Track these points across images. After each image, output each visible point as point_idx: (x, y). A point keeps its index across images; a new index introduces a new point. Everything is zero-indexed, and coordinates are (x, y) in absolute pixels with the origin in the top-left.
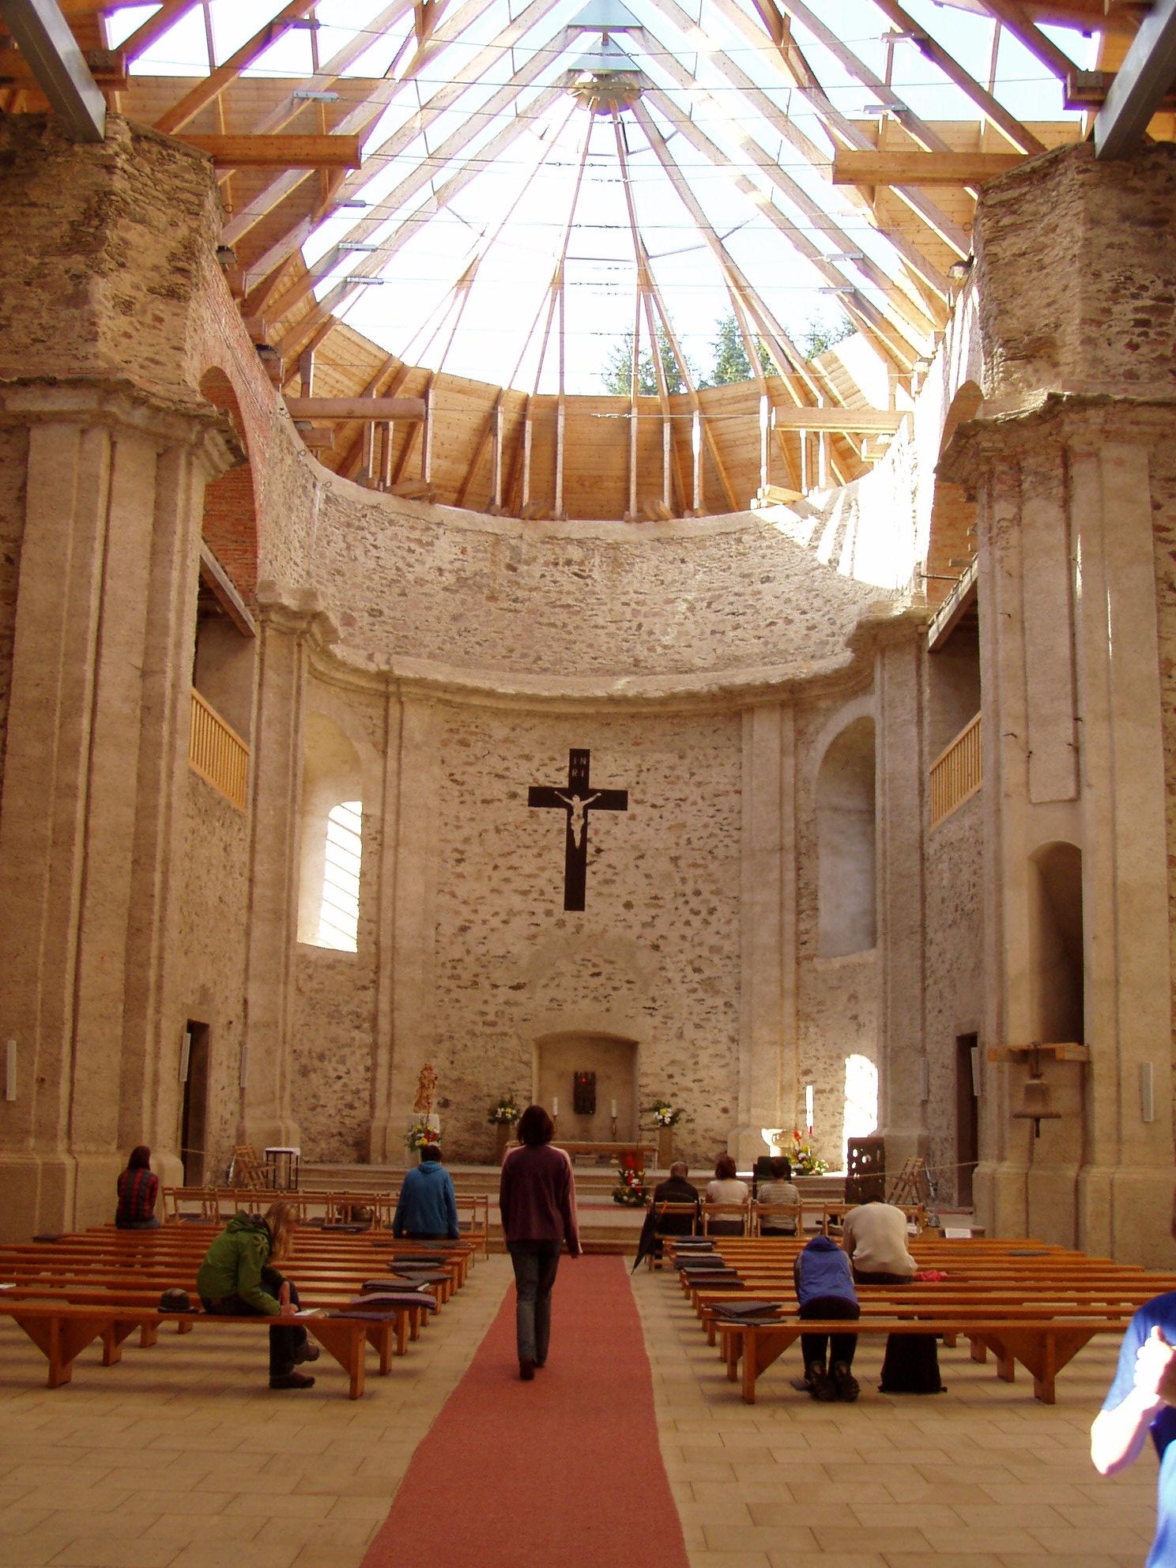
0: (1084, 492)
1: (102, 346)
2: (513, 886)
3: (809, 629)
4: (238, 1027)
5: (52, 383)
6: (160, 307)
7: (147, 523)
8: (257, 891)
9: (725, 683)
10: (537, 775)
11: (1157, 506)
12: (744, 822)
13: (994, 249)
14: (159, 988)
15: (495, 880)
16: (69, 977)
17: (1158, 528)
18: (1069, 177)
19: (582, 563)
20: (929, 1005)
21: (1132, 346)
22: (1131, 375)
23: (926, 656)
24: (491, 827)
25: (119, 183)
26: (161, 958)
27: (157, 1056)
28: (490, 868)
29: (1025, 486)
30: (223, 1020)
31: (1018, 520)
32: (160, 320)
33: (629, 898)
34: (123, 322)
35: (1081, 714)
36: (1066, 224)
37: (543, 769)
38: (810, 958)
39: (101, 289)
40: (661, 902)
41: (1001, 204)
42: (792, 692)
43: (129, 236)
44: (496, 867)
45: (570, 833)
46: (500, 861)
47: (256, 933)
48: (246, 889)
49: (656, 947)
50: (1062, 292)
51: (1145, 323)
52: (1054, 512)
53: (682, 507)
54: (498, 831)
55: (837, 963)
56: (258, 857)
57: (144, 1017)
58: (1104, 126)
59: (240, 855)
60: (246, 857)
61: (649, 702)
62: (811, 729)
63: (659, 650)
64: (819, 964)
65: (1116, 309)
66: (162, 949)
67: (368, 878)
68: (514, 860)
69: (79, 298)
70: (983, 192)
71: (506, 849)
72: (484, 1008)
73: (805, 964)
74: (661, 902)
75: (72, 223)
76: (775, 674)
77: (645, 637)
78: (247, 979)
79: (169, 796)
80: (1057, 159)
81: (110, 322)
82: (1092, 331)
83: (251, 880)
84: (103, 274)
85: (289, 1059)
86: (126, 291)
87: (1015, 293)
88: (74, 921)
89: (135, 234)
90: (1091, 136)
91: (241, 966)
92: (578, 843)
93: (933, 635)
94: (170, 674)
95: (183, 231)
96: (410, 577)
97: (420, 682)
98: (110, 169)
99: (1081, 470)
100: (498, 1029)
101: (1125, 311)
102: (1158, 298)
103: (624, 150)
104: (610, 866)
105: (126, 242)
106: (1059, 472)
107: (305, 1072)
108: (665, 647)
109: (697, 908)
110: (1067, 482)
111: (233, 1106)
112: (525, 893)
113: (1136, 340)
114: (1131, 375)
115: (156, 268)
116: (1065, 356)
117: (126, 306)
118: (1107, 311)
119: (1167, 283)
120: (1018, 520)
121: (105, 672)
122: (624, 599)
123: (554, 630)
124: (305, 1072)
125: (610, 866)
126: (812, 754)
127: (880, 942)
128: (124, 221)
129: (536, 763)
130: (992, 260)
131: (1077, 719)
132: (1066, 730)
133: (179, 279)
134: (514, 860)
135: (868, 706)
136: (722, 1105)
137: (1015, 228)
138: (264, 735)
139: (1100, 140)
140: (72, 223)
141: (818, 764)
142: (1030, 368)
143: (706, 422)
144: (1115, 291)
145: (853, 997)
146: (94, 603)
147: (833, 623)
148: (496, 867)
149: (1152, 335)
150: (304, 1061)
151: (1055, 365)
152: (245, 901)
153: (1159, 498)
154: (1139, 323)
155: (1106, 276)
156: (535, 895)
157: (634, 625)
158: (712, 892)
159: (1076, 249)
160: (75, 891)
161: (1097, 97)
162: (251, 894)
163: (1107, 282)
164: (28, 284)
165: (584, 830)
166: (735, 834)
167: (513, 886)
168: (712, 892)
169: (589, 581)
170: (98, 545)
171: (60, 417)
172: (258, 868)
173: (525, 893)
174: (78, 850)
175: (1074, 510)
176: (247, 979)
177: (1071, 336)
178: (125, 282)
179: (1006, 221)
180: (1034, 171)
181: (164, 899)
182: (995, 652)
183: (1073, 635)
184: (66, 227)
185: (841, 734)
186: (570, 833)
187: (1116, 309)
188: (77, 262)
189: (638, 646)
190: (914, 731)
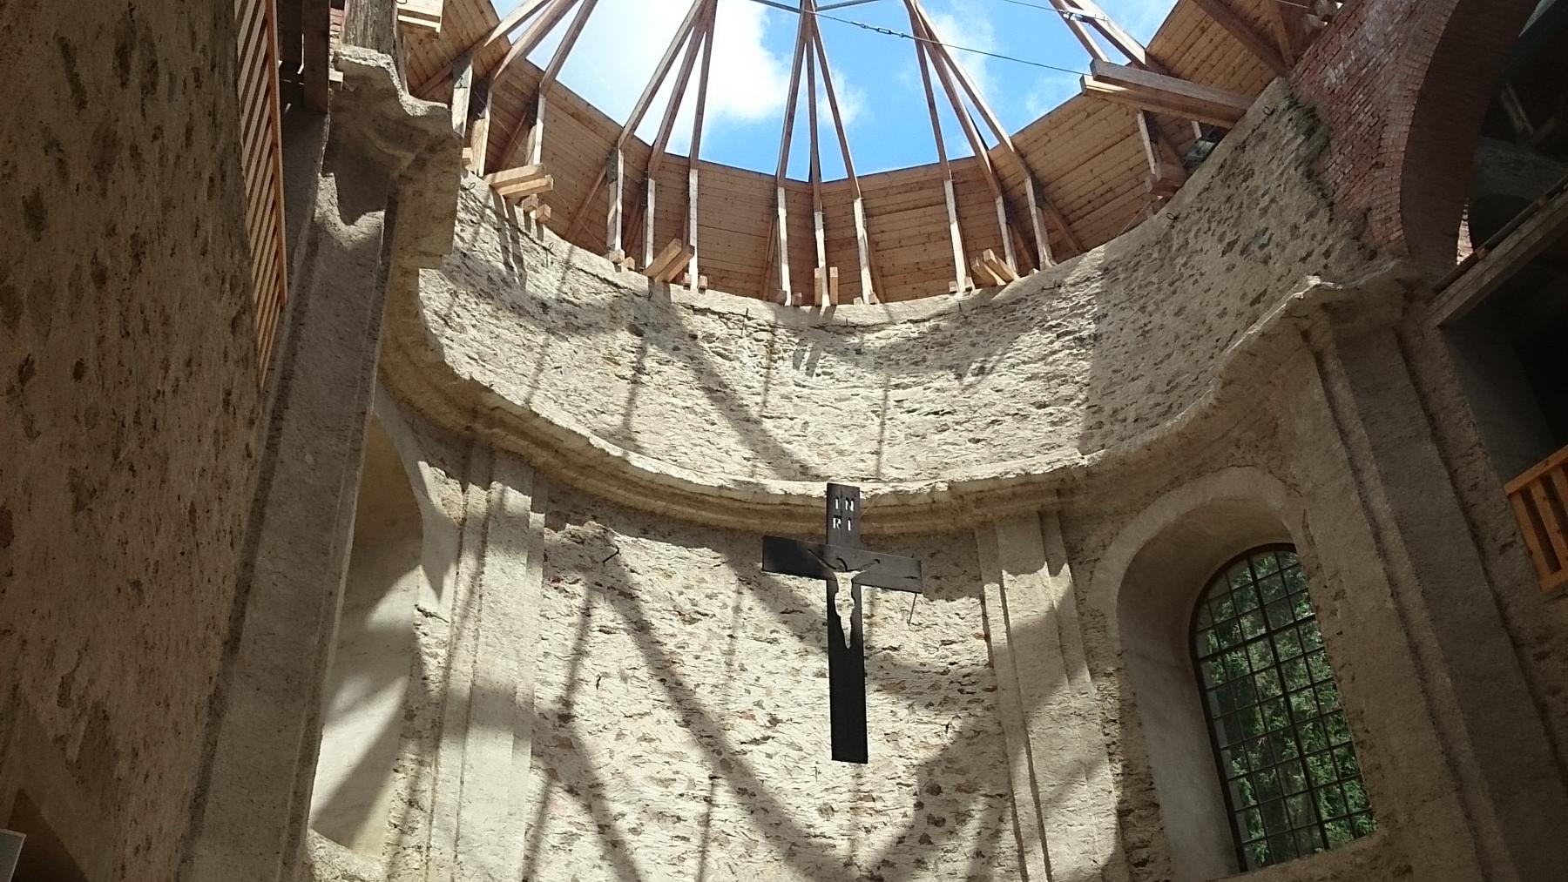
2: (647, 770)
3: (1053, 424)
8: (253, 615)
10: (680, 600)
12: (1000, 676)
15: (618, 757)
19: (725, 341)
24: (613, 671)
28: (611, 736)
33: (828, 798)
37: (691, 594)
40: (879, 805)
42: (1059, 492)
44: (620, 736)
46: (628, 726)
53: (849, 292)
54: (624, 679)
56: (267, 537)
62: (1092, 541)
63: (834, 455)
67: (417, 723)
68: (646, 726)
71: (635, 709)
74: (879, 805)
77: (813, 439)
78: (194, 830)
92: (847, 631)
104: (791, 745)
108: (841, 453)
109: (937, 814)
112: (665, 783)
122: (783, 390)
123: (691, 416)
125: (791, 745)
126: (1099, 575)
129: (678, 580)
134: (646, 726)
141: (1115, 589)
147: (1101, 410)
148: (620, 736)
156: (679, 788)
157: (799, 422)
158: (959, 789)
162: (237, 618)
166: (989, 698)
167: (647, 770)
168: (959, 789)
169: (737, 364)
172: (261, 561)
173: (665, 783)
176: (194, 830)
189: (806, 450)
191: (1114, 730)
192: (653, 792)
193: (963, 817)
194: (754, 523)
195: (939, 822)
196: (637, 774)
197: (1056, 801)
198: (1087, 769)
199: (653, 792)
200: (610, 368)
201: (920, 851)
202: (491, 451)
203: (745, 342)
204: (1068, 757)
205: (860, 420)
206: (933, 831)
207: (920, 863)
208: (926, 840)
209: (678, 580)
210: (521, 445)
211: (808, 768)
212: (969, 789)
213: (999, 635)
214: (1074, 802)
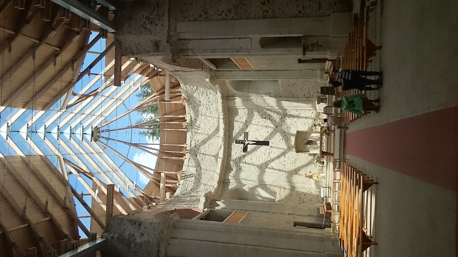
0: (187, 36)
1: (151, 240)
4: (294, 216)
5: (159, 250)
6: (142, 227)
7: (189, 230)
9: (221, 111)
11: (190, 21)
13: (135, 53)
14: (287, 231)
16: (285, 250)
17: (195, 21)
18: (121, 38)
19: (196, 141)
20: (291, 69)
21: (156, 25)
22: (163, 25)
23: (218, 69)
25: (116, 236)
26: (281, 230)
27: (302, 232)
29: (185, 48)
30: (293, 219)
31: (192, 50)
32: (145, 227)
33: (266, 132)
34: (146, 235)
35: (233, 37)
36: (130, 39)
38: (280, 94)
39: (138, 240)
41: (126, 51)
43: (127, 234)
45: (253, 144)
46: (258, 159)
47: (274, 211)
48: (264, 213)
49: (277, 127)
50: (145, 40)
51: (152, 22)
52: (191, 42)
53: (184, 120)
55: (281, 89)
57: (294, 235)
58: (111, 30)
59: (257, 214)
60: (258, 213)
61: (225, 127)
62: (231, 93)
64: (281, 93)
65: (149, 28)
66: (279, 230)
68: (258, 156)
69: (141, 245)
70: (123, 55)
72: (289, 163)
73: (281, 95)
75: (124, 246)
76: (220, 101)
79: (246, 227)
80: (117, 40)
81: (145, 238)
82: (153, 34)
83: (263, 212)
84: (135, 240)
85: (301, 205)
86: (139, 234)
87: (145, 49)
88: (274, 249)
89: (127, 233)
90: (112, 33)
91: (281, 215)
93: (214, 68)
94: (221, 227)
95: (126, 222)
96: (198, 177)
97: (220, 175)
98: (113, 238)
99: (182, 36)
100: (294, 161)
101: (149, 26)
102: (146, 19)
103: (109, 131)
105: (129, 235)
106: (183, 41)
107: (304, 202)
110: (185, 40)
111: (312, 218)
113: (155, 24)
114: (163, 25)
115: (134, 228)
116: (158, 39)
117: (142, 234)
118: (149, 30)
119: (143, 17)
120: (192, 50)
121: (220, 240)
124: (304, 202)
127: (278, 80)
128: (124, 235)
129: (237, 151)
130: (137, 54)
131: (234, 38)
132: (237, 40)
133: (137, 223)
134: (258, 156)
135: (227, 81)
136: (311, 113)
137: (131, 49)
138: (231, 208)
139: (113, 31)
140: (124, 246)
142: (161, 47)
143: (165, 115)
144: (145, 28)
145: (289, 85)
146: (205, 242)
149: (154, 21)
150: (301, 202)
151: (160, 41)
152: (267, 213)
153: (188, 20)
154: (152, 24)
155: (142, 30)
159: (136, 36)
160: (267, 248)
161: (105, 31)
163: (143, 30)
164: (137, 256)
165: (252, 141)
170: (193, 241)
171: (166, 249)
173: (265, 154)
174: (258, 248)
175: (190, 38)
177: (154, 38)
178: (137, 235)
179: (130, 51)
180: (119, 45)
181: (268, 229)
182: (220, 55)
183: (216, 39)
184: (125, 247)
185: (233, 87)
186: (253, 144)
187: (149, 28)
188: (132, 245)
190: (233, 72)
191: (259, 95)
192: (266, 156)
193: (269, 115)
194: (227, 139)
195: (270, 118)
196: (264, 158)
197: (268, 104)
198: (264, 100)
199: (266, 156)
200: (204, 160)
201: (273, 121)
202: (224, 179)
203: (195, 138)
204: (263, 102)
205: (208, 121)
206: (271, 119)
207: (275, 121)
208: (272, 120)
209: (237, 151)
210: (223, 175)
211: (262, 134)
212: (266, 113)
213: (244, 107)
214: (268, 103)
